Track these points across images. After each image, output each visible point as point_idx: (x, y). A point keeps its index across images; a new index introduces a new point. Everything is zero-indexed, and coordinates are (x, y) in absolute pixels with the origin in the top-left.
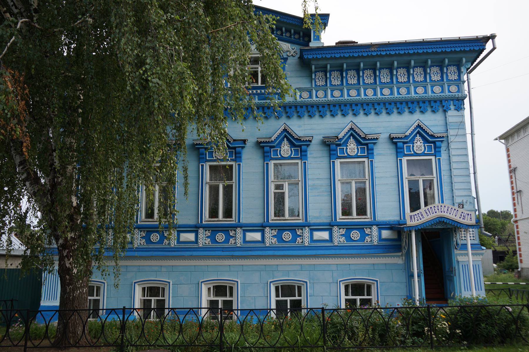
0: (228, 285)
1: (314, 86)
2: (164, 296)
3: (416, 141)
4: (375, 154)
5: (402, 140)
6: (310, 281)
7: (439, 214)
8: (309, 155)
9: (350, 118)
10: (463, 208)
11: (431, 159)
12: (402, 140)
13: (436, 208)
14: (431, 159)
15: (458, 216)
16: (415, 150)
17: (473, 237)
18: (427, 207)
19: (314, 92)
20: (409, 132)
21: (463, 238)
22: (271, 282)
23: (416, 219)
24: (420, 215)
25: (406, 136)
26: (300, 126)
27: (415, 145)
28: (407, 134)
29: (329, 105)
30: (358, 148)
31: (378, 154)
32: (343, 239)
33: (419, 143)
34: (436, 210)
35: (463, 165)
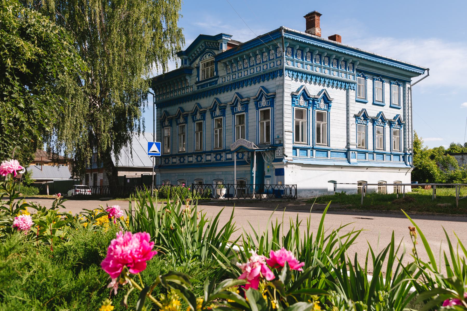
1: (226, 74)
8: (226, 114)
11: (269, 110)
14: (269, 109)
15: (247, 145)
20: (257, 95)
25: (257, 97)
28: (257, 96)
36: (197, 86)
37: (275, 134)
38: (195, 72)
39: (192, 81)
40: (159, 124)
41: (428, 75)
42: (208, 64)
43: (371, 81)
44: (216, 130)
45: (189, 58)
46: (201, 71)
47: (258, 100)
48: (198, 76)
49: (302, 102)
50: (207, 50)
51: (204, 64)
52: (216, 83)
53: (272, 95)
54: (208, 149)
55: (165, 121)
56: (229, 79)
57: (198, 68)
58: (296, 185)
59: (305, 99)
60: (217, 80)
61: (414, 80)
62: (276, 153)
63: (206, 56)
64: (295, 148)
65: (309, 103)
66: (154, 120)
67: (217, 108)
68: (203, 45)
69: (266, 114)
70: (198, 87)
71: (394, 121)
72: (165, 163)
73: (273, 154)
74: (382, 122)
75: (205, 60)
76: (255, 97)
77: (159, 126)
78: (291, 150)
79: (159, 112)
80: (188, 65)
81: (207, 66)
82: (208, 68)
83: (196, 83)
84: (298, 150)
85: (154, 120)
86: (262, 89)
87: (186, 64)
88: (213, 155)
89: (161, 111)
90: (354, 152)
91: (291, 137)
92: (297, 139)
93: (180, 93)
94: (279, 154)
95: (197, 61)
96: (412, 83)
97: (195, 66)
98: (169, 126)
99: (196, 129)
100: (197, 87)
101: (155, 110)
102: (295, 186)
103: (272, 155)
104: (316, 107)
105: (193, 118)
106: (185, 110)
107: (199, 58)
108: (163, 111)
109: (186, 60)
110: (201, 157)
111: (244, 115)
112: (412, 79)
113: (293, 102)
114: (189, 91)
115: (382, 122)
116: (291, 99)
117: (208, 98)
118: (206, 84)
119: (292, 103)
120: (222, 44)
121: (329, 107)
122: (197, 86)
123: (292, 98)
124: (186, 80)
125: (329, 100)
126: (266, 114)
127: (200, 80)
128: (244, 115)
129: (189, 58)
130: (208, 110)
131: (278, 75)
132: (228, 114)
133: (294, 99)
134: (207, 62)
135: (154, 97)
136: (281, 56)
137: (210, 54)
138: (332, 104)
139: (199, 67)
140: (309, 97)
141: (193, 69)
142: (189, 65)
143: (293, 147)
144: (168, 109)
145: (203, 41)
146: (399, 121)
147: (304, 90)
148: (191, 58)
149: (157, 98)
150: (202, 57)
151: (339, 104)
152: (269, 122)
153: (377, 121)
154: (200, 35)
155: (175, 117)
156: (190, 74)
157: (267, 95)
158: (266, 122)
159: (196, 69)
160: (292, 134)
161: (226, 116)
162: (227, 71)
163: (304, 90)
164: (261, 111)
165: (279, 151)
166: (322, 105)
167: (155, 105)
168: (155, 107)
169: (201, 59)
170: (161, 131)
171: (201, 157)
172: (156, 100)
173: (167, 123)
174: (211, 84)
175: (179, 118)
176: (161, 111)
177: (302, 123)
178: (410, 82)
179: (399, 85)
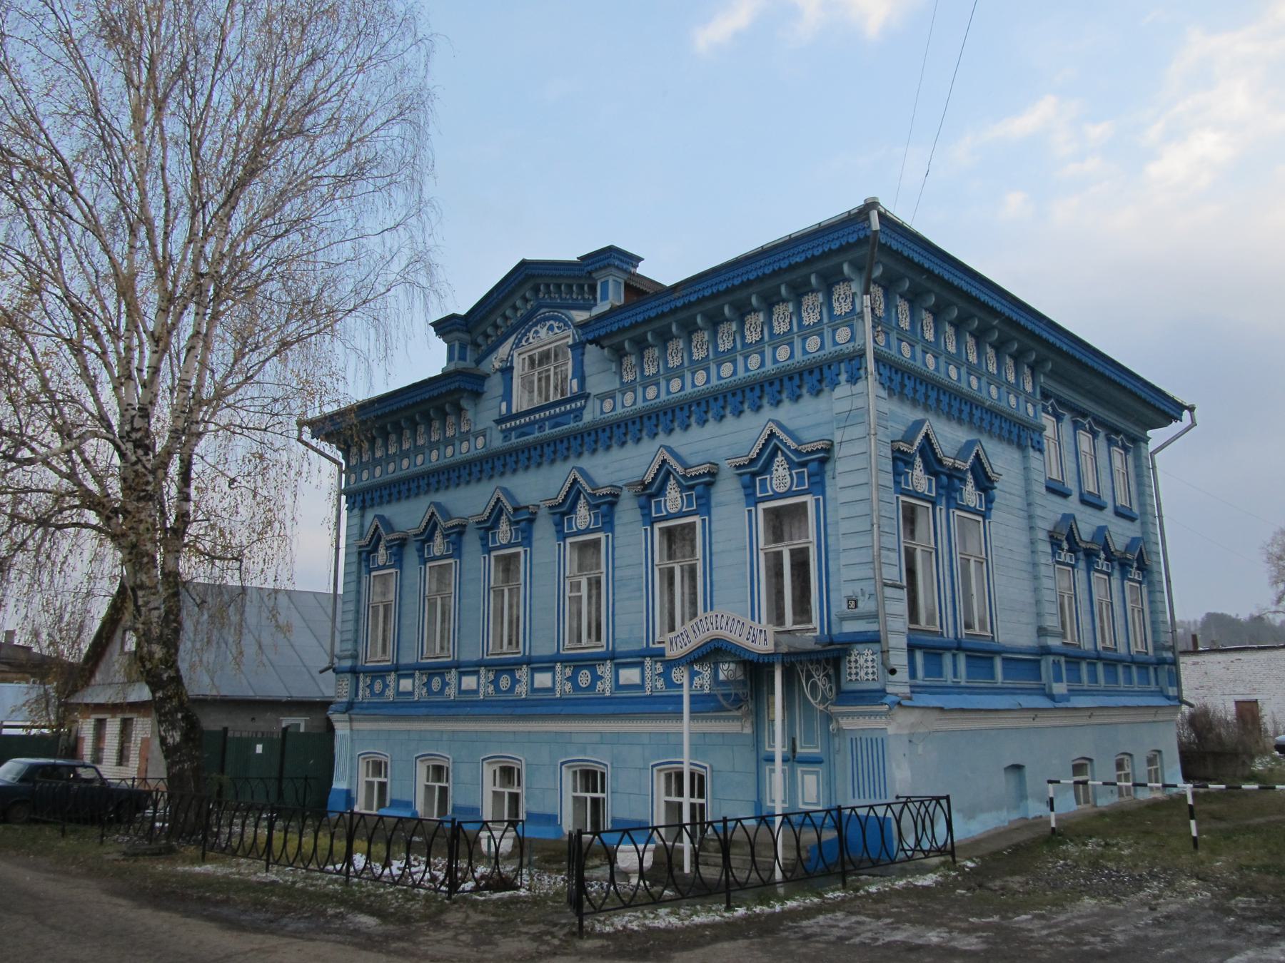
0: (516, 767)
1: (617, 385)
3: (775, 467)
4: (713, 504)
5: (749, 470)
6: (612, 764)
7: (714, 633)
9: (662, 439)
10: (856, 607)
11: (805, 503)
12: (749, 470)
13: (709, 622)
14: (805, 503)
16: (774, 487)
17: (873, 673)
18: (693, 622)
19: (619, 396)
20: (755, 451)
21: (854, 677)
22: (562, 764)
23: (679, 644)
24: (685, 637)
26: (606, 468)
27: (775, 475)
28: (754, 454)
29: (641, 417)
30: (682, 497)
31: (720, 504)
32: (660, 683)
33: (780, 469)
34: (709, 624)
35: (861, 509)
36: (502, 431)
37: (832, 595)
38: (494, 386)
40: (354, 558)
42: (545, 357)
44: (576, 579)
48: (507, 396)
49: (920, 479)
50: (543, 310)
51: (531, 358)
53: (818, 451)
54: (544, 648)
55: (375, 549)
56: (629, 403)
57: (507, 371)
58: (947, 798)
59: (929, 470)
60: (583, 408)
63: (537, 332)
64: (912, 648)
66: (337, 549)
67: (582, 502)
68: (528, 295)
70: (506, 434)
72: (373, 694)
73: (831, 672)
75: (531, 347)
77: (354, 568)
79: (356, 521)
80: (468, 364)
81: (540, 364)
82: (545, 367)
83: (499, 422)
85: (337, 549)
87: (463, 358)
89: (362, 516)
94: (862, 674)
95: (504, 350)
97: (497, 365)
98: (390, 567)
99: (495, 576)
100: (501, 436)
101: (344, 513)
102: (944, 802)
103: (827, 675)
104: (956, 499)
105: (484, 540)
106: (454, 513)
107: (512, 339)
108: (370, 515)
109: (463, 347)
110: (513, 677)
111: (693, 525)
116: (890, 468)
117: (545, 469)
118: (535, 422)
120: (605, 284)
121: (990, 501)
122: (502, 431)
123: (894, 459)
124: (459, 411)
125: (988, 478)
127: (514, 411)
128: (693, 525)
130: (543, 512)
131: (843, 377)
132: (624, 525)
133: (900, 464)
134: (540, 350)
135: (341, 472)
136: (853, 309)
137: (556, 324)
139: (511, 368)
140: (940, 461)
141: (483, 378)
142: (473, 365)
143: (909, 645)
144: (388, 511)
145: (530, 284)
148: (480, 340)
149: (353, 477)
150: (525, 334)
151: (1008, 496)
152: (805, 551)
154: (524, 264)
155: (416, 535)
156: (477, 395)
158: (791, 551)
159: (499, 374)
161: (618, 529)
162: (621, 377)
163: (927, 435)
164: (765, 510)
165: (861, 661)
167: (344, 498)
168: (344, 506)
169: (520, 341)
170: (359, 582)
171: (513, 677)
172: (347, 482)
173: (382, 555)
174: (556, 421)
175: (430, 538)
176: (362, 516)
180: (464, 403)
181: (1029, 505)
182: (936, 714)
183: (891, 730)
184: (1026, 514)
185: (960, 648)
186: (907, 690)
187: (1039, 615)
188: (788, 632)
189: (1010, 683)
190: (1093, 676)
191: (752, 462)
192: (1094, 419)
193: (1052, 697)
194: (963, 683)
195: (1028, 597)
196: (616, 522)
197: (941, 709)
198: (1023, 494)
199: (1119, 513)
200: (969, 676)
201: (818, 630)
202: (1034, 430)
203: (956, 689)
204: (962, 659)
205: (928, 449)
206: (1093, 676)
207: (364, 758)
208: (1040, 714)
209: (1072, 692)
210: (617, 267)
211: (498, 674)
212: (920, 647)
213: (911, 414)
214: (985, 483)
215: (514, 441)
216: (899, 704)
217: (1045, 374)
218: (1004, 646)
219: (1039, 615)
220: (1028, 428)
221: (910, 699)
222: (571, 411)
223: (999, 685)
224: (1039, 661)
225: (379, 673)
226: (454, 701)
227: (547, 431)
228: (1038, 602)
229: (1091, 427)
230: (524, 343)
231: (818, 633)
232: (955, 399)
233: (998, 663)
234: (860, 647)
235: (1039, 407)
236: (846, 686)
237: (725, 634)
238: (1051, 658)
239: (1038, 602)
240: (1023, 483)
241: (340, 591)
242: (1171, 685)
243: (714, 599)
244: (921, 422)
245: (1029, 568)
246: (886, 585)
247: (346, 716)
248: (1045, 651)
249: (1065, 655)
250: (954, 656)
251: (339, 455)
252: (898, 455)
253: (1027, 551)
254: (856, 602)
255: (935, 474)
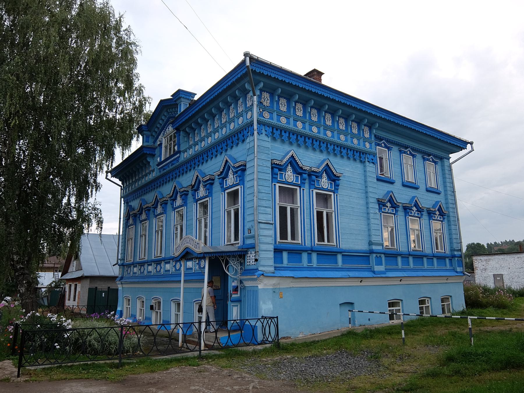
2: (443, 305)
10: (251, 233)
36: (159, 169)
39: (153, 163)
41: (473, 150)
43: (398, 153)
45: (152, 135)
46: (163, 149)
47: (223, 175)
49: (289, 175)
52: (178, 161)
58: (277, 317)
59: (295, 171)
60: (179, 157)
61: (453, 157)
62: (247, 259)
63: (169, 128)
64: (278, 251)
65: (303, 179)
66: (120, 218)
69: (234, 196)
71: (433, 210)
74: (417, 211)
76: (219, 173)
78: (271, 255)
80: (150, 143)
84: (285, 255)
85: (120, 218)
86: (228, 159)
88: (173, 263)
90: (378, 255)
91: (272, 232)
92: (284, 235)
93: (144, 181)
94: (251, 262)
96: (451, 161)
101: (123, 205)
102: (276, 319)
109: (148, 137)
112: (450, 155)
113: (274, 176)
114: (153, 175)
115: (417, 211)
119: (272, 178)
126: (234, 196)
129: (152, 135)
133: (276, 170)
135: (121, 189)
138: (341, 183)
140: (301, 168)
142: (153, 144)
146: (440, 209)
147: (292, 156)
151: (352, 183)
152: (238, 209)
153: (410, 210)
157: (234, 167)
160: (271, 227)
163: (292, 156)
164: (228, 193)
166: (325, 182)
167: (122, 199)
168: (123, 202)
169: (164, 133)
177: (292, 210)
178: (449, 158)
179: (435, 163)
180: (149, 159)
181: (366, 187)
182: (291, 280)
183: (260, 287)
184: (364, 191)
185: (312, 251)
186: (272, 269)
187: (370, 235)
188: (232, 244)
189: (291, 265)
190: (310, 260)
191: (222, 173)
192: (412, 149)
193: (374, 272)
194: (315, 266)
195: (364, 227)
196: (188, 202)
197: (293, 277)
198: (363, 182)
199: (429, 190)
200: (318, 262)
201: (240, 243)
202: (369, 154)
203: (310, 268)
204: (314, 256)
205: (293, 162)
206: (310, 260)
207: (126, 298)
208: (364, 280)
209: (387, 270)
210: (184, 98)
211: (157, 264)
212: (286, 250)
213: (287, 147)
214: (334, 178)
215: (162, 172)
216: (263, 275)
217: (376, 129)
218: (343, 249)
219: (370, 235)
220: (366, 154)
221: (274, 273)
222: (176, 158)
223: (340, 267)
224: (369, 256)
225: (129, 266)
226: (146, 276)
227: (170, 167)
228: (369, 230)
229: (410, 153)
230: (165, 133)
231: (240, 245)
232: (316, 141)
233: (340, 257)
234: (251, 250)
235: (373, 144)
236: (247, 268)
237: (188, 245)
238: (374, 255)
239: (369, 230)
240: (363, 178)
241: (121, 233)
242: (459, 266)
243: (213, 232)
244: (290, 151)
245: (365, 215)
246: (260, 223)
247: (120, 282)
248: (372, 252)
249: (384, 254)
250: (310, 254)
251: (120, 183)
252: (273, 165)
253: (365, 208)
254: (250, 230)
255: (300, 174)
